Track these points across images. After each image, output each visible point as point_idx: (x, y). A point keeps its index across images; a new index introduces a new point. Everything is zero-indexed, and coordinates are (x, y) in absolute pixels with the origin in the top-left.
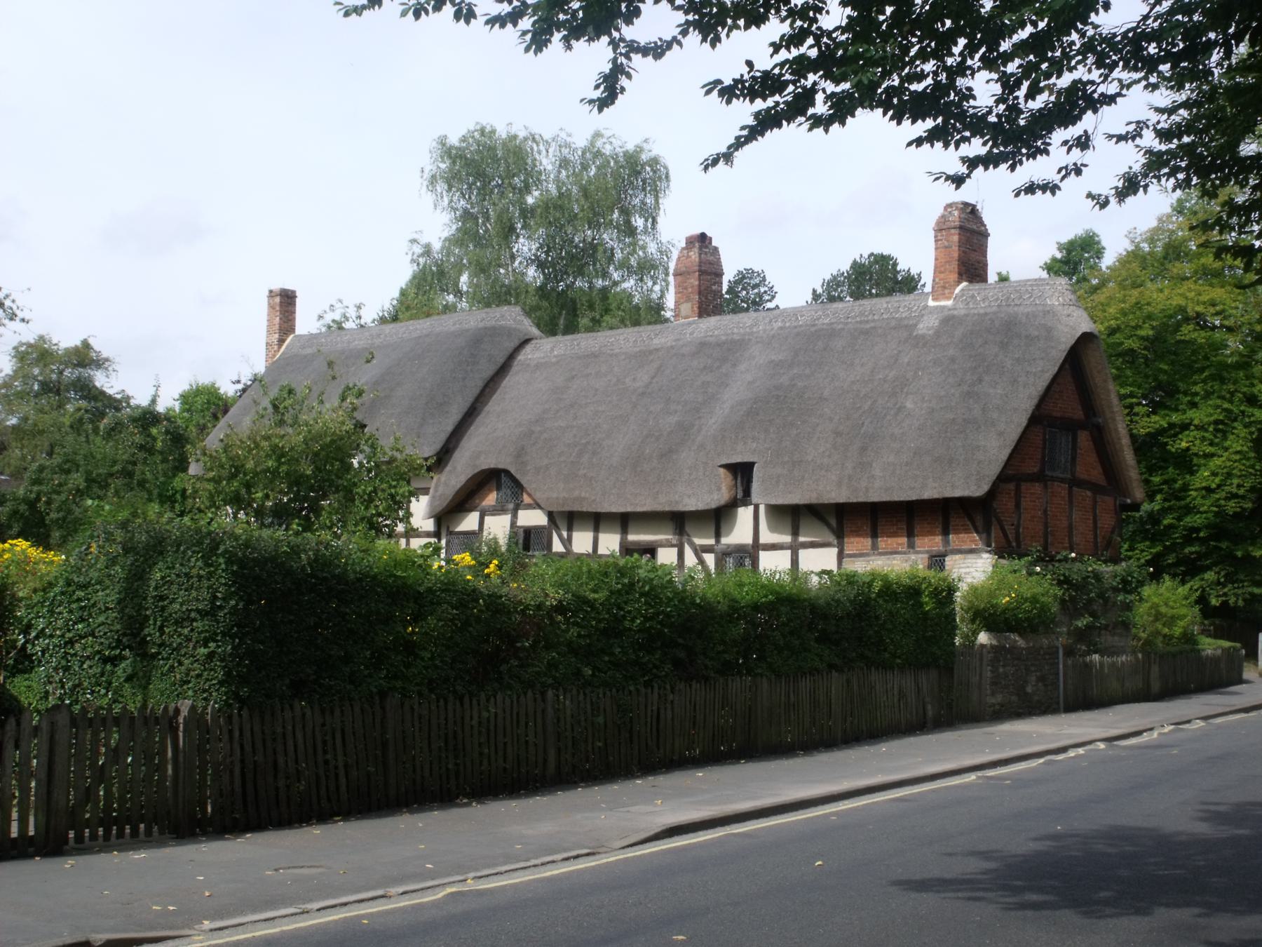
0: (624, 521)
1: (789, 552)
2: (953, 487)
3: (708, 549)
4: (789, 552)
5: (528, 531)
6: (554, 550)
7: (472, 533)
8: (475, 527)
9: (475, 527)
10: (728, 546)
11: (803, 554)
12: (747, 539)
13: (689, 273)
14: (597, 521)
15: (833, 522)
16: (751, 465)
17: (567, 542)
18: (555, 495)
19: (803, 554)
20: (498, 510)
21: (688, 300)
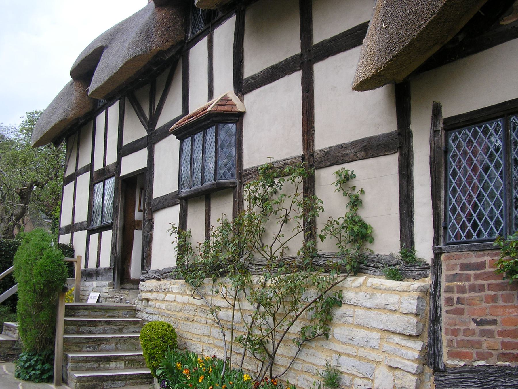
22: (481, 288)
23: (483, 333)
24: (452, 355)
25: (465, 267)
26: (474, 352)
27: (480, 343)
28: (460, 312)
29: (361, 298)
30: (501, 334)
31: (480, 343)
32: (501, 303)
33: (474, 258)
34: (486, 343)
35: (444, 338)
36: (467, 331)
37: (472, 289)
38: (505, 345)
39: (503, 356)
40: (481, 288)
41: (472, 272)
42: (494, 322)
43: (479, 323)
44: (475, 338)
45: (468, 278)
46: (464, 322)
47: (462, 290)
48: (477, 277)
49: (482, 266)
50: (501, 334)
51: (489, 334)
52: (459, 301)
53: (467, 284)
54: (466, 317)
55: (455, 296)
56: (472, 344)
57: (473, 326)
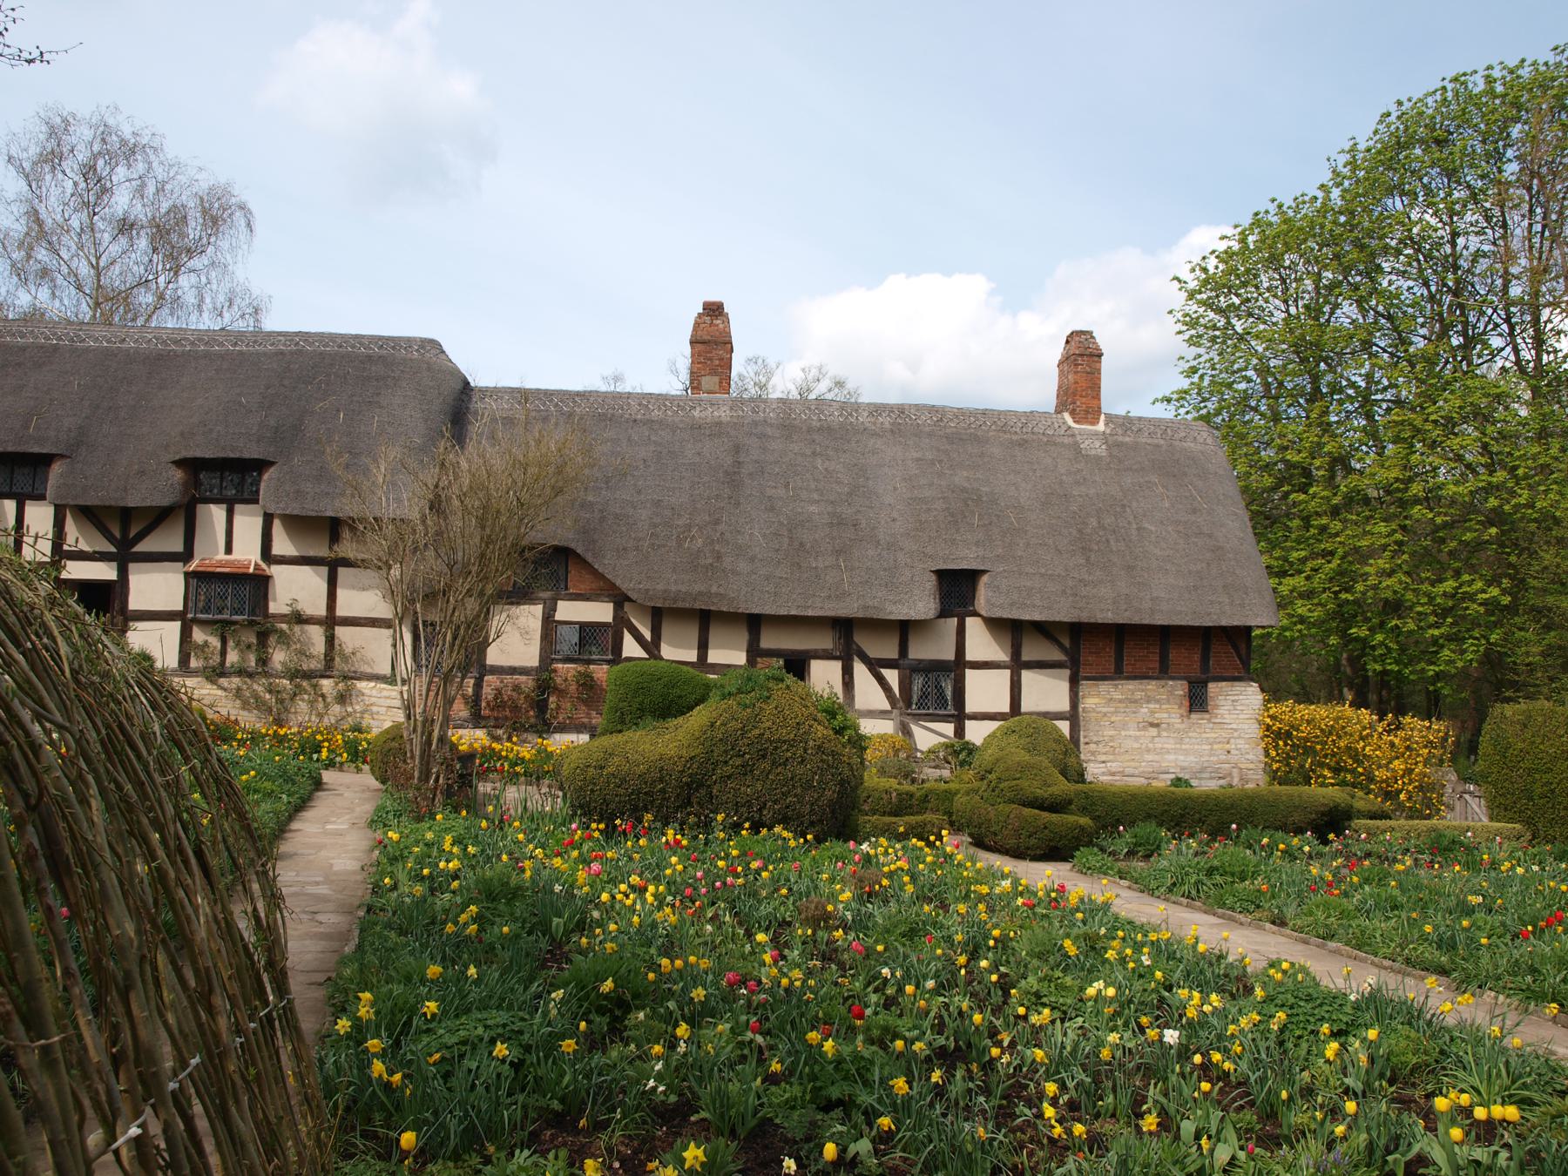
0: (754, 623)
1: (1007, 672)
2: (1257, 616)
3: (890, 664)
4: (1007, 672)
5: (583, 626)
10: (920, 661)
11: (1027, 676)
12: (950, 655)
13: (716, 343)
14: (705, 620)
15: (1067, 643)
16: (984, 572)
17: (652, 648)
18: (660, 587)
19: (1027, 676)
20: (519, 595)
21: (713, 372)
29: (374, 693)
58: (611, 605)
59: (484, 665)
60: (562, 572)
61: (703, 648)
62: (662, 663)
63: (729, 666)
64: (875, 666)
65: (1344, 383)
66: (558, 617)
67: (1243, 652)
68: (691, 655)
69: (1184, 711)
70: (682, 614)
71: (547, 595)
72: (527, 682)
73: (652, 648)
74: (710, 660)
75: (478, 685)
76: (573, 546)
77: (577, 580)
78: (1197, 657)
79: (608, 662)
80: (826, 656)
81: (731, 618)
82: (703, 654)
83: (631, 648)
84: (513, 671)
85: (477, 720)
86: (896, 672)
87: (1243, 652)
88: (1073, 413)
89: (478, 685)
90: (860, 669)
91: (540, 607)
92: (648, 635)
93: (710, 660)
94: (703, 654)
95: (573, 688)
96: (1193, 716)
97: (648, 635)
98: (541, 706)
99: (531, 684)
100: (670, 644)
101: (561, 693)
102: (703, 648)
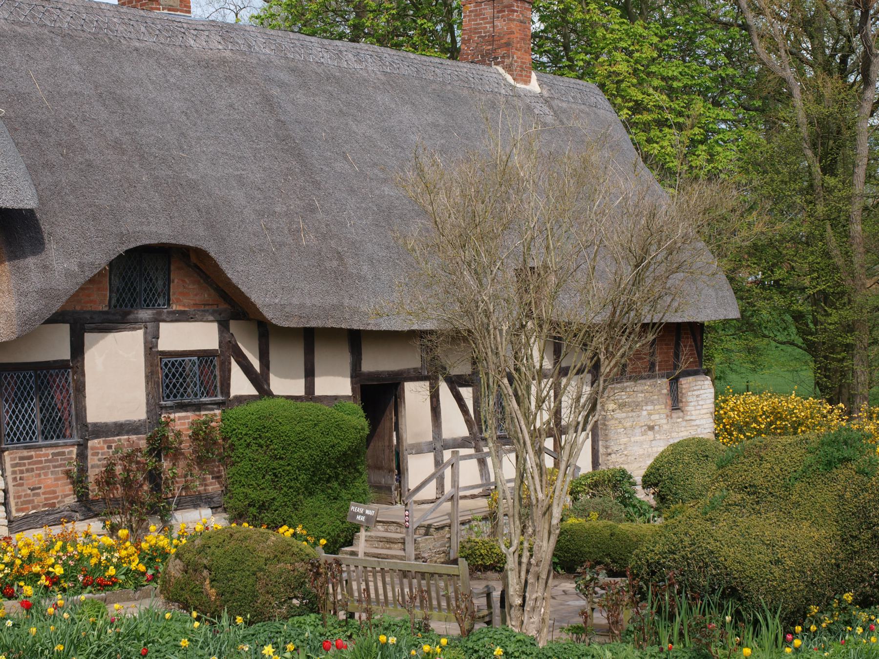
0: (355, 340)
6: (234, 392)
7: (62, 365)
8: (67, 356)
9: (66, 355)
14: (310, 340)
18: (295, 301)
20: (113, 321)
22: (32, 470)
23: (34, 495)
24: (18, 510)
25: (21, 458)
26: (30, 506)
27: (33, 501)
28: (21, 485)
30: (44, 493)
31: (33, 501)
32: (43, 477)
33: (25, 453)
34: (36, 500)
35: (12, 502)
36: (26, 495)
37: (28, 471)
38: (46, 499)
39: (45, 505)
40: (32, 470)
41: (26, 461)
42: (40, 488)
43: (32, 490)
44: (31, 498)
45: (24, 465)
46: (24, 491)
47: (22, 472)
48: (29, 464)
49: (30, 457)
50: (44, 493)
51: (38, 495)
52: (21, 479)
53: (24, 468)
54: (25, 487)
55: (18, 477)
56: (29, 502)
57: (29, 491)
58: (215, 326)
59: (85, 425)
60: (160, 283)
61: (310, 375)
62: (277, 400)
63: (336, 398)
64: (455, 383)
65: (810, 73)
66: (161, 347)
67: (699, 344)
68: (296, 387)
69: (668, 411)
70: (288, 334)
71: (145, 314)
72: (141, 441)
73: (259, 380)
74: (319, 392)
75: (82, 456)
76: (204, 245)
77: (184, 290)
78: (672, 352)
79: (219, 404)
80: (417, 377)
81: (332, 335)
82: (310, 387)
83: (240, 385)
84: (120, 428)
85: (87, 507)
86: (470, 389)
87: (699, 344)
88: (509, 69)
89: (82, 456)
90: (444, 389)
91: (140, 333)
92: (256, 364)
93: (319, 392)
94: (310, 387)
95: (186, 446)
96: (674, 415)
97: (256, 364)
98: (154, 477)
99: (143, 444)
100: (276, 375)
101: (177, 454)
102: (310, 375)
